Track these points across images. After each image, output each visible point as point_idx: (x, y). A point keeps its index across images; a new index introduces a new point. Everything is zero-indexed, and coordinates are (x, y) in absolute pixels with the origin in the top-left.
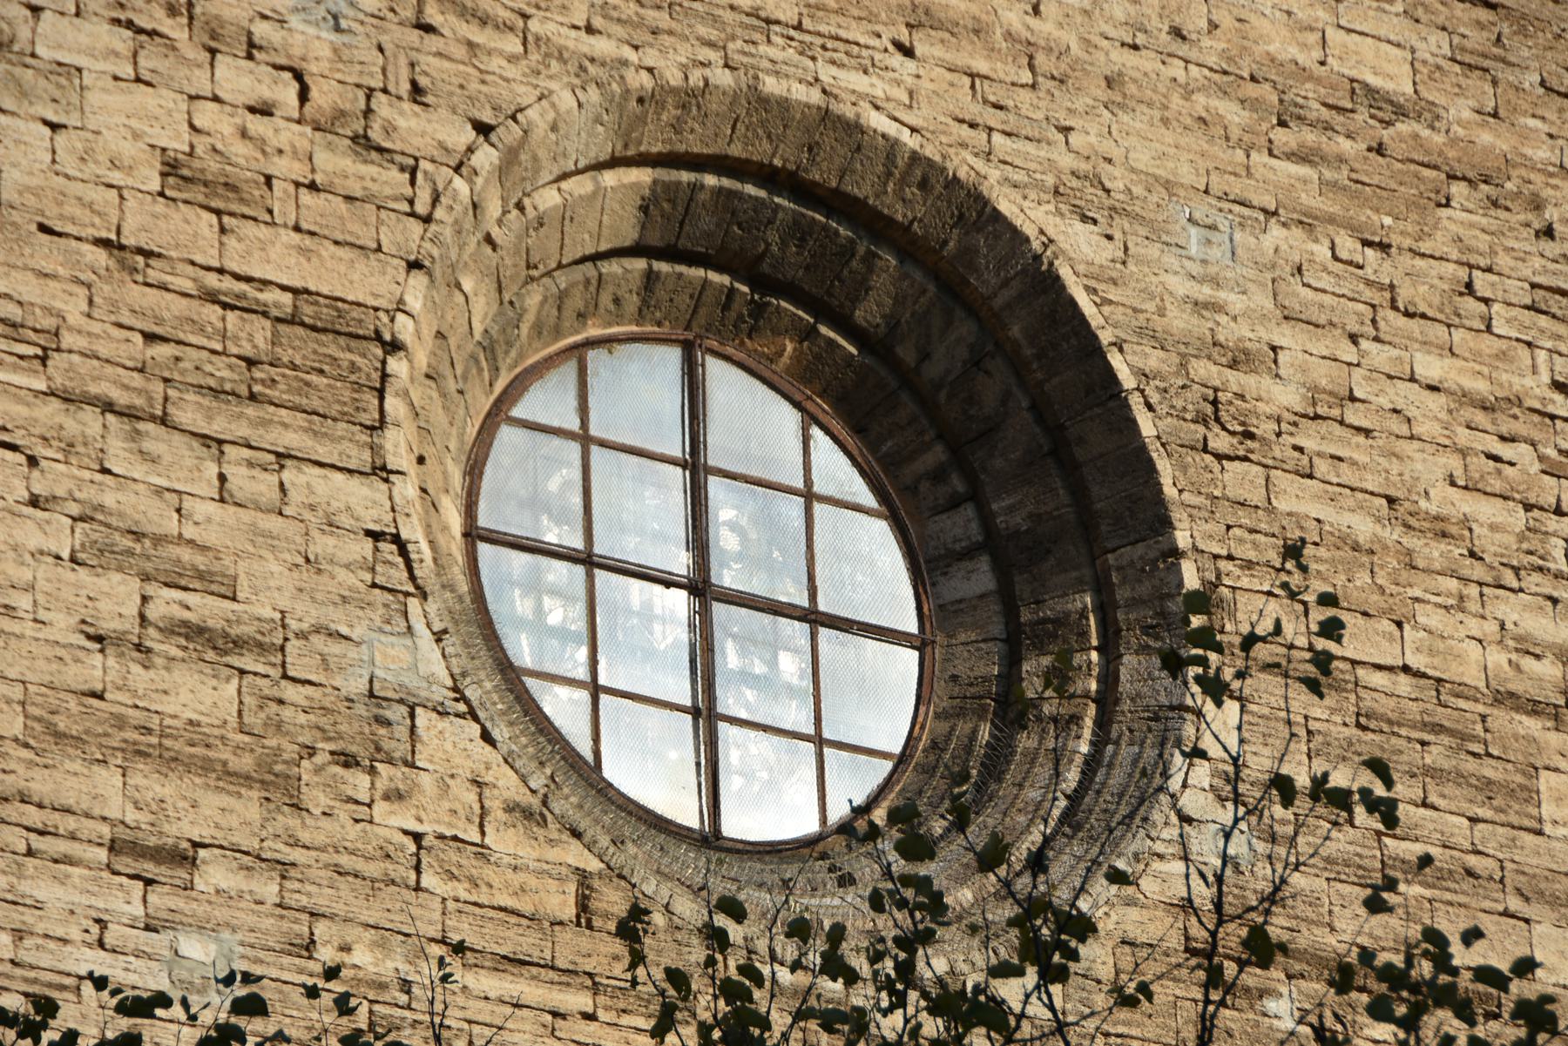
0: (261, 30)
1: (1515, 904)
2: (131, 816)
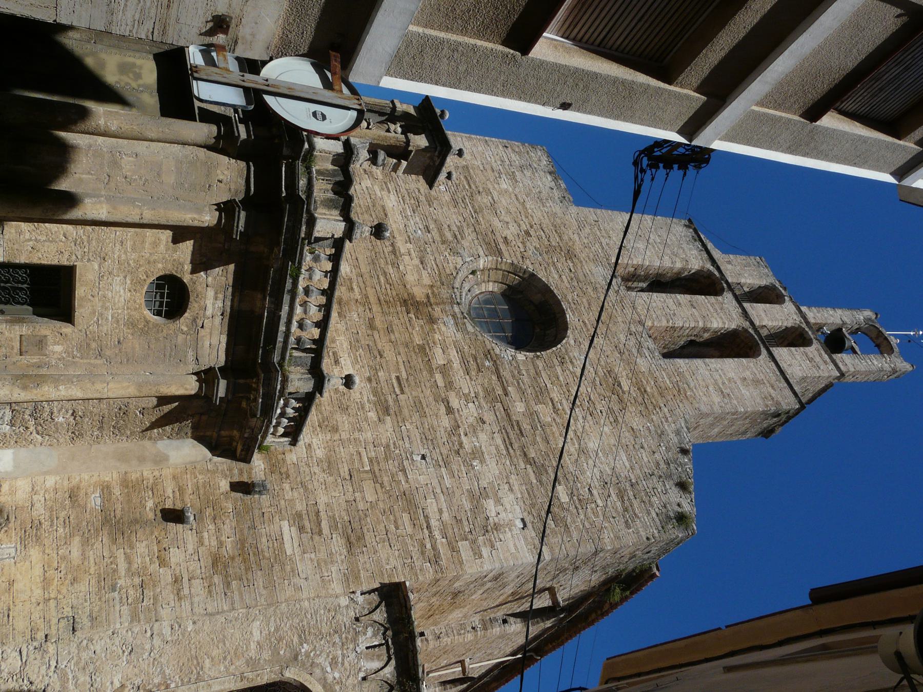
0: (527, 248)
1: (523, 400)
2: (431, 228)
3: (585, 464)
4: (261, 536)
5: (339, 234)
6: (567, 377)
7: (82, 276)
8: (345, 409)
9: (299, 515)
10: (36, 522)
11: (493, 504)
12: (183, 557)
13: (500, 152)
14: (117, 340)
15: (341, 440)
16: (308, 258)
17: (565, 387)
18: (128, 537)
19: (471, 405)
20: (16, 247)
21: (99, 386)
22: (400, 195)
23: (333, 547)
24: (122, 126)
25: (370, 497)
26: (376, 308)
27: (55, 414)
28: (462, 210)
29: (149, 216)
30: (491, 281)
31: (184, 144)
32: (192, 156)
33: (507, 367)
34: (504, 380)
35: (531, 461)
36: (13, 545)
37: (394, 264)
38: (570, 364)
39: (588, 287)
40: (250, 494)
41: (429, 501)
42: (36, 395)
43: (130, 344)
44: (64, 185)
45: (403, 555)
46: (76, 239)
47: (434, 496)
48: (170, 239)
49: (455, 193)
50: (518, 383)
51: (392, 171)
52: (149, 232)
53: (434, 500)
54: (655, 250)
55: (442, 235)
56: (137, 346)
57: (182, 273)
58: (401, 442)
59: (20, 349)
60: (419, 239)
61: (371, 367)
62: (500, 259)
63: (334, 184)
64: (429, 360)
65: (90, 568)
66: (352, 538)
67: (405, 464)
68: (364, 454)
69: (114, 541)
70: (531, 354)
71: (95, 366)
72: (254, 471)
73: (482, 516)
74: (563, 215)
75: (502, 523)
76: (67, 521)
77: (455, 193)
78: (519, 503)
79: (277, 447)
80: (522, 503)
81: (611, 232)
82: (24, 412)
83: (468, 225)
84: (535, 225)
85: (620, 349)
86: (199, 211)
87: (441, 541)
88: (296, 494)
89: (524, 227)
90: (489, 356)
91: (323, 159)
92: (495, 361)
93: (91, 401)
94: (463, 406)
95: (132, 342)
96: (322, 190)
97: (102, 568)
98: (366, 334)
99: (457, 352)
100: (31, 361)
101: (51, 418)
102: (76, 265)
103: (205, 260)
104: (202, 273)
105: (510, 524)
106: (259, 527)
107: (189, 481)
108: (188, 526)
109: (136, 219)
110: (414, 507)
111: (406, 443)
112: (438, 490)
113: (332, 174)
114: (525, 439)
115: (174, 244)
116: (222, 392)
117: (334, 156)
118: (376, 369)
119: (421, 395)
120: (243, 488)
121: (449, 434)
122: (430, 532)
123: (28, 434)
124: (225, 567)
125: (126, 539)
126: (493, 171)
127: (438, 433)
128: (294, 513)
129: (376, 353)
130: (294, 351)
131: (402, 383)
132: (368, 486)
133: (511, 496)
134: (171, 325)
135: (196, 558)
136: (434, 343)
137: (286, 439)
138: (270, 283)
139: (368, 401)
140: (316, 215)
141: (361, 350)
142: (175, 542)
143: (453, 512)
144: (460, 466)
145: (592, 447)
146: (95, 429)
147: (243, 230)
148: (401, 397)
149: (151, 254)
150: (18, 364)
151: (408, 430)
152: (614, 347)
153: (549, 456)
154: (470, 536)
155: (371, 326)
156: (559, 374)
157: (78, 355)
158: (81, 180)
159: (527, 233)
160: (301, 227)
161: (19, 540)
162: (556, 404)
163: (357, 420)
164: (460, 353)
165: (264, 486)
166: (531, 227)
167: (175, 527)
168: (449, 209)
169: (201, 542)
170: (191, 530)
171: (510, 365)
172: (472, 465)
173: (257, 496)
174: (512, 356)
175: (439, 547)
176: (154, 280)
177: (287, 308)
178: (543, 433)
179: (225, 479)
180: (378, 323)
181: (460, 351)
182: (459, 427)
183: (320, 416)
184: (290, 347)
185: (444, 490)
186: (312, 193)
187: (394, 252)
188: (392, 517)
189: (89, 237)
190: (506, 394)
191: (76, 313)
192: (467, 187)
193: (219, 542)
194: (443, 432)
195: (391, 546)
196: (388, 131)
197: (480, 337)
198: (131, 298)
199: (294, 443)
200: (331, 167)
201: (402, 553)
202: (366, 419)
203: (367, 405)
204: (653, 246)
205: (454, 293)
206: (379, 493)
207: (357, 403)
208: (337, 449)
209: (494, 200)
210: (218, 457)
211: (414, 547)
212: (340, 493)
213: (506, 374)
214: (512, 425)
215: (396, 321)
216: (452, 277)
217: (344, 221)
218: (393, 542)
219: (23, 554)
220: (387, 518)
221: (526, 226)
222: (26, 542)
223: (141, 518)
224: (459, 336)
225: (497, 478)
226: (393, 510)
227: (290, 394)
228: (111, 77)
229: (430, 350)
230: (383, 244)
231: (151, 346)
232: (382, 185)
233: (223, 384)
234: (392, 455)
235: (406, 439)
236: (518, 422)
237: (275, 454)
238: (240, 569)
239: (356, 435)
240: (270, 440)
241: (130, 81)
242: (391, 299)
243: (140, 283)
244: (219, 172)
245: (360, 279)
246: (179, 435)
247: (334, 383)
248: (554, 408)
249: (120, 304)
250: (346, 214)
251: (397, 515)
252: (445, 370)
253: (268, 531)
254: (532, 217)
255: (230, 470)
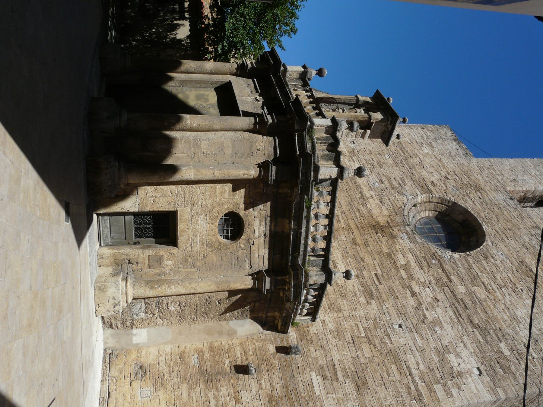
1: (463, 284)
2: (384, 180)
3: (517, 327)
4: (298, 383)
5: (334, 176)
6: (491, 267)
7: (182, 217)
8: (344, 296)
9: (322, 368)
10: (161, 374)
11: (454, 357)
12: (250, 397)
13: (419, 132)
14: (203, 256)
15: (344, 317)
16: (316, 194)
17: (491, 274)
18: (215, 384)
19: (427, 289)
20: (145, 201)
21: (194, 285)
22: (361, 163)
23: (347, 390)
24: (200, 123)
25: (368, 354)
26: (356, 232)
27: (170, 305)
28: (401, 168)
29: (218, 174)
30: (427, 210)
31: (236, 130)
32: (241, 137)
33: (448, 263)
34: (447, 272)
35: (476, 326)
36: (149, 389)
37: (363, 204)
38: (491, 258)
39: (494, 207)
40: (289, 354)
41: (408, 356)
42: (159, 292)
43: (211, 258)
44: (170, 161)
45: (396, 395)
46: (177, 194)
47: (412, 352)
48: (231, 189)
49: (395, 158)
50: (457, 273)
51: (361, 138)
52: (218, 186)
53: (412, 356)
54: (537, 180)
55: (391, 184)
56: (215, 259)
57: (239, 210)
58: (384, 317)
59: (149, 264)
60: (377, 188)
61: (358, 269)
62: (431, 195)
63: (327, 145)
64: (395, 262)
65: (193, 404)
66: (359, 383)
67: (388, 331)
68: (360, 325)
69: (207, 386)
70: (463, 253)
71: (191, 273)
72: (290, 339)
73: (448, 366)
74: (468, 165)
75: (463, 371)
76: (179, 373)
77: (395, 158)
78: (473, 356)
79: (303, 323)
80: (475, 356)
81: (503, 172)
82: (152, 304)
83: (407, 177)
84: (450, 173)
85: (526, 246)
86: (248, 169)
87: (421, 385)
88: (318, 354)
89: (443, 174)
90: (434, 257)
91: (320, 131)
92: (439, 260)
93: (189, 295)
94: (422, 291)
95: (212, 257)
96: (321, 149)
97: (201, 404)
98: (351, 248)
99: (413, 255)
100: (155, 272)
101: (168, 308)
102: (178, 210)
103: (252, 201)
104: (251, 209)
105: (470, 372)
106: (297, 377)
107: (250, 346)
108: (252, 376)
109: (209, 177)
110: (399, 361)
111: (387, 317)
112: (414, 349)
113: (326, 139)
114: (469, 311)
115: (233, 192)
116: (268, 286)
117: (326, 128)
118: (361, 270)
119: (393, 285)
120: (284, 350)
121: (415, 310)
122: (413, 378)
123: (155, 318)
124: (277, 404)
125: (214, 385)
126: (417, 143)
127: (408, 309)
128: (318, 366)
129: (360, 260)
130: (310, 257)
131: (379, 277)
132: (366, 347)
133: (467, 352)
134: (234, 244)
135: (258, 398)
136: (396, 251)
137: (309, 317)
138: (294, 212)
139: (359, 290)
140: (319, 165)
141: (350, 258)
142: (244, 387)
143: (427, 364)
144: (426, 331)
145: (520, 315)
146: (192, 314)
147: (274, 178)
148: (380, 287)
149: (220, 199)
150: (148, 274)
151: (387, 308)
152: (521, 245)
153: (489, 322)
154: (441, 381)
155: (354, 243)
156: (485, 265)
157: (181, 267)
158: (178, 157)
159: (446, 178)
160: (311, 172)
161: (152, 384)
162: (487, 286)
163: (353, 303)
164: (414, 256)
165: (297, 348)
166: (448, 174)
167: (243, 377)
168: (393, 168)
169: (260, 387)
170: (254, 379)
171: (449, 262)
172: (434, 330)
173: (293, 356)
174: (450, 256)
175: (420, 388)
176: (222, 216)
177: (305, 228)
178: (481, 306)
179: (272, 344)
180: (358, 240)
181: (414, 255)
182: (422, 305)
183: (328, 302)
184: (308, 254)
185: (418, 348)
186: (315, 152)
187: (362, 197)
188: (384, 368)
189: (184, 192)
190: (450, 281)
191: (179, 240)
192: (402, 154)
193: (271, 387)
194: (411, 309)
195: (386, 389)
196: (356, 112)
197: (426, 245)
198: (210, 229)
199: (314, 319)
200: (324, 135)
201: (395, 394)
202: (359, 302)
203: (358, 293)
204: (536, 178)
205: (405, 219)
206: (373, 351)
207: (351, 292)
208: (342, 323)
209: (421, 160)
210: (267, 330)
211: (403, 389)
212: (347, 352)
213: (448, 268)
214: (458, 301)
215: (370, 239)
216: (401, 209)
217: (337, 167)
218: (388, 386)
219: (155, 395)
220: (381, 369)
221: (445, 173)
222: (156, 387)
223: (222, 371)
224: (412, 245)
225: (454, 339)
226: (385, 363)
227: (311, 285)
228: (192, 102)
229: (395, 255)
230: (355, 193)
231: (223, 258)
232: (349, 159)
233: (268, 280)
234: (379, 325)
235: (387, 314)
236: (462, 300)
237: (302, 328)
238: (287, 405)
239: (354, 313)
240: (299, 318)
241: (202, 103)
242: (365, 225)
243: (215, 218)
244: (257, 144)
245: (344, 215)
246: (242, 317)
247: (338, 277)
248: (486, 288)
249: (203, 233)
250: (337, 162)
251: (388, 366)
252: (406, 267)
253: (302, 379)
254: (448, 167)
255: (275, 339)
